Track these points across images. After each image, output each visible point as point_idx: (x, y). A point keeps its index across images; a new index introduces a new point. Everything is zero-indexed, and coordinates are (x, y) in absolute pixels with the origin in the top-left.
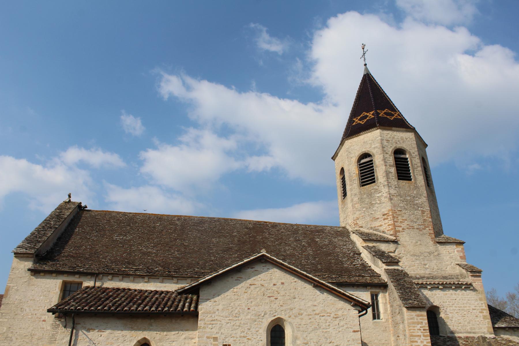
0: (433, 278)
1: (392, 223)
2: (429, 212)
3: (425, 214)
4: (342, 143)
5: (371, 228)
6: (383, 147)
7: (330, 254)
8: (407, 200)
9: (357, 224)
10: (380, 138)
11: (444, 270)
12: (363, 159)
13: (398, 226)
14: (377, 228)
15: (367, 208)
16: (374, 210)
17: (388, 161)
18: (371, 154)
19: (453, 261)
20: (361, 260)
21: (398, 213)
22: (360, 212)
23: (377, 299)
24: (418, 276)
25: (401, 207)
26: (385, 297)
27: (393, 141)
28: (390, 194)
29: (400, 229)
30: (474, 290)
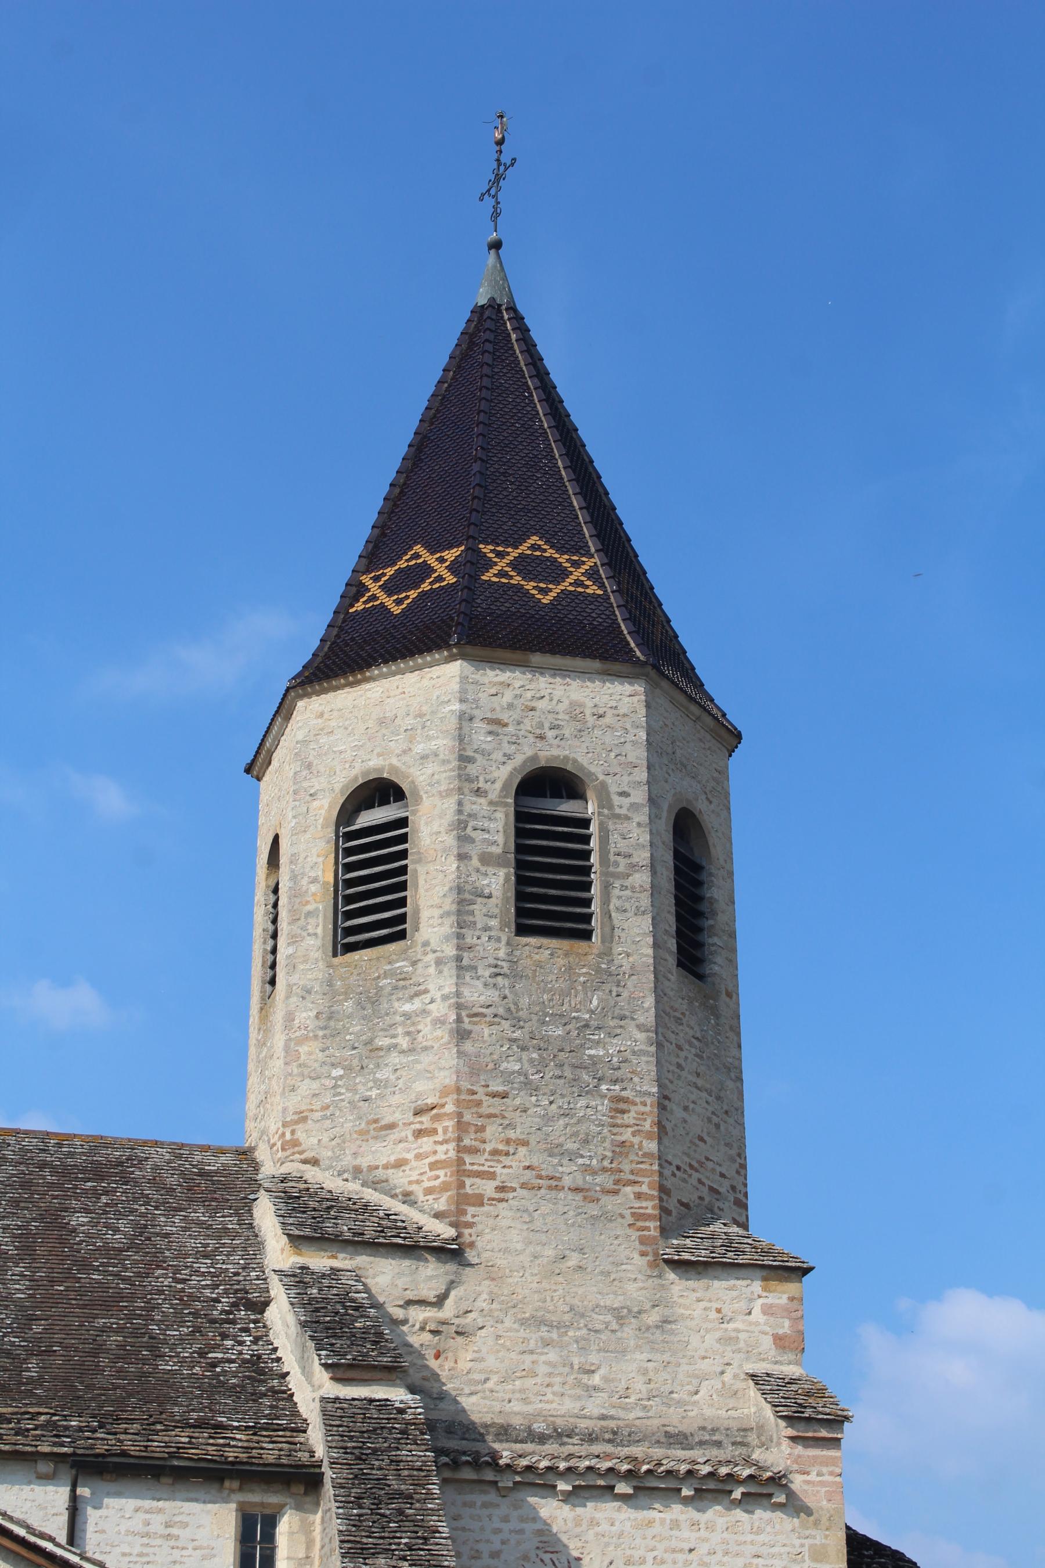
0: (614, 1437)
1: (452, 1154)
2: (649, 1107)
3: (629, 1118)
4: (284, 711)
5: (357, 1171)
6: (465, 759)
7: (109, 1303)
8: (546, 1039)
9: (295, 1143)
10: (456, 706)
11: (679, 1403)
12: (369, 805)
13: (479, 1174)
14: (380, 1173)
15: (349, 1069)
16: (378, 1083)
17: (478, 836)
18: (405, 787)
19: (737, 1359)
20: (255, 1341)
21: (490, 1105)
22: (315, 1085)
23: (269, 1537)
24: (539, 1427)
25: (508, 1077)
26: (306, 1529)
27: (527, 725)
28: (459, 1007)
29: (488, 1188)
30: (794, 1506)
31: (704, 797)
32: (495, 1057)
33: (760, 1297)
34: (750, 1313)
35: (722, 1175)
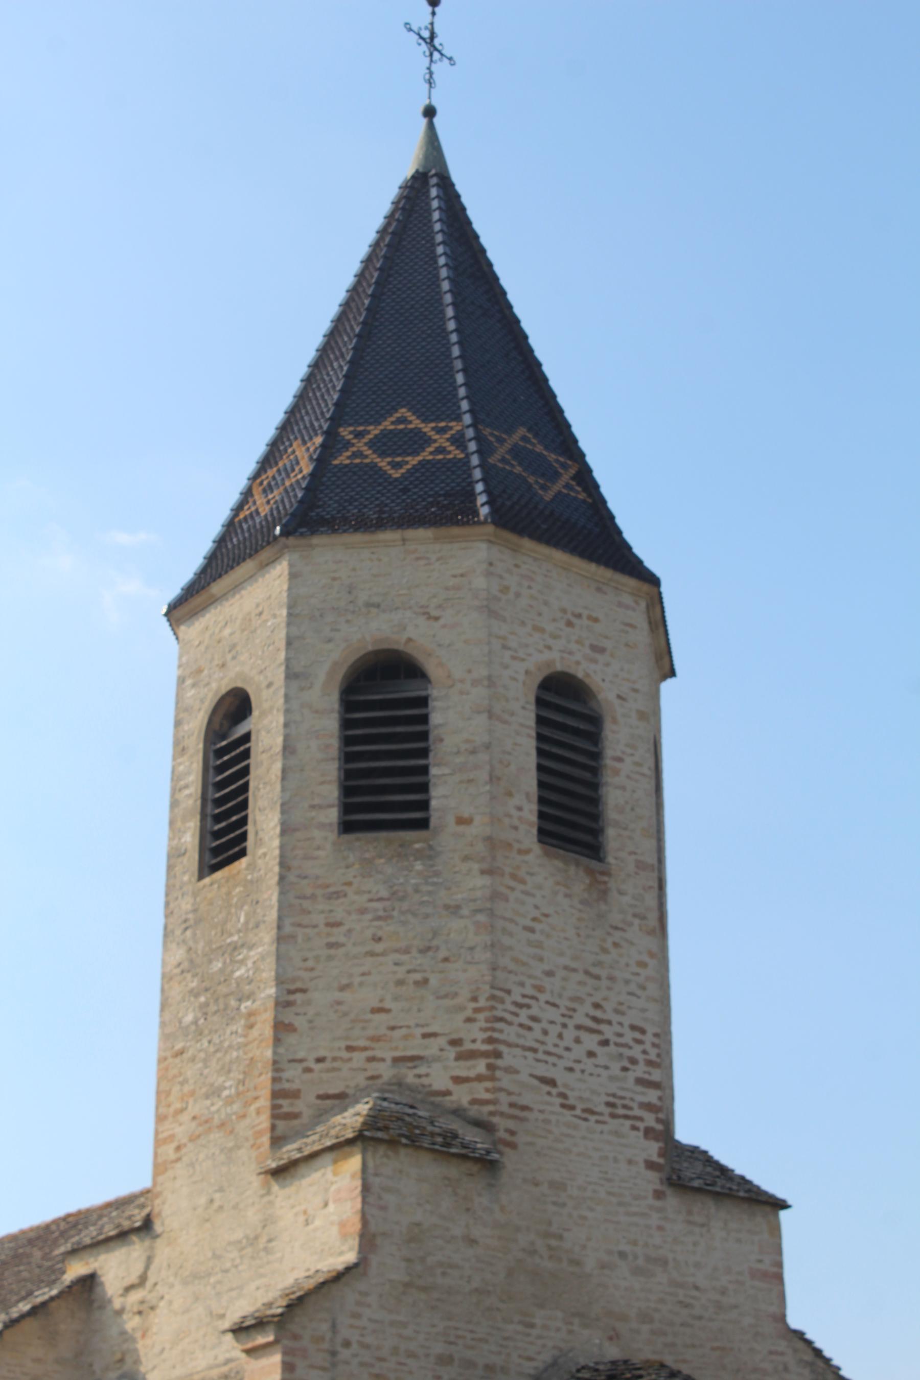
3: (255, 1033)
31: (421, 620)
32: (180, 1015)
33: (332, 1183)
34: (326, 1205)
35: (425, 1036)
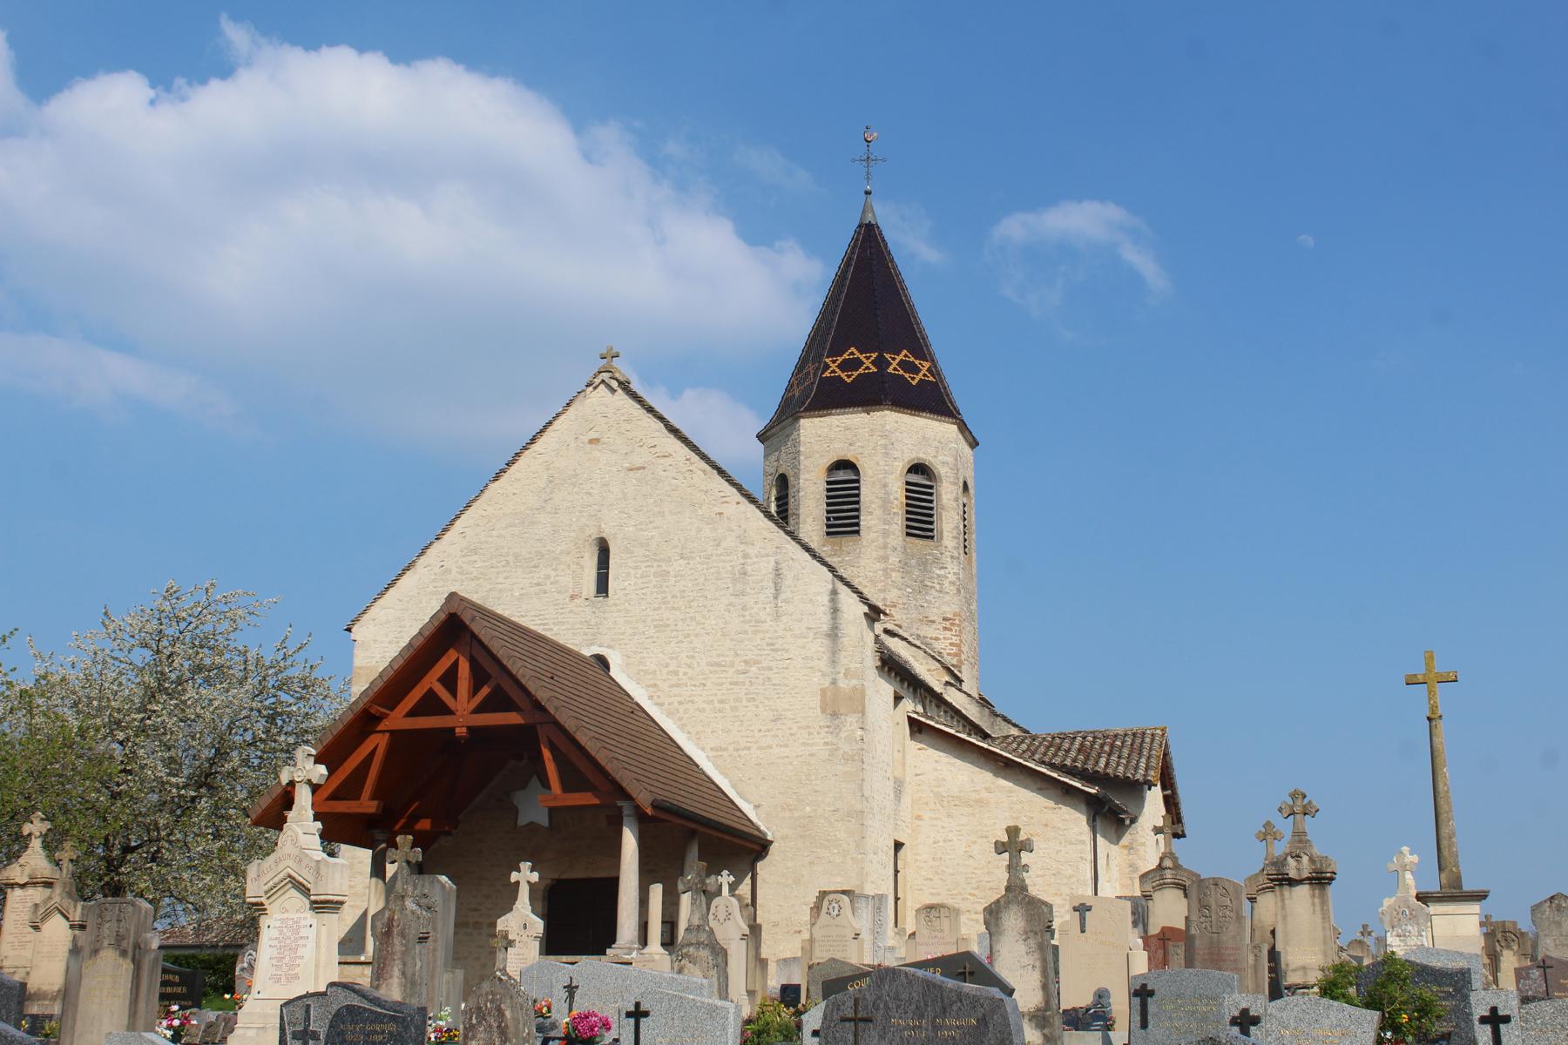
16: (929, 602)
